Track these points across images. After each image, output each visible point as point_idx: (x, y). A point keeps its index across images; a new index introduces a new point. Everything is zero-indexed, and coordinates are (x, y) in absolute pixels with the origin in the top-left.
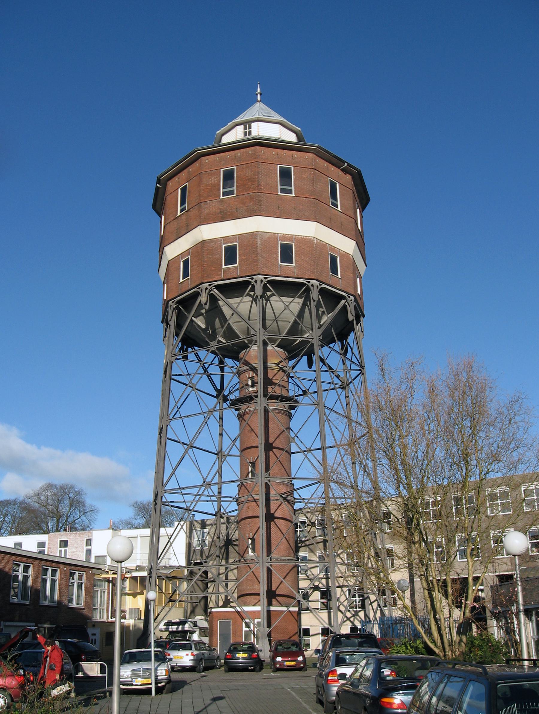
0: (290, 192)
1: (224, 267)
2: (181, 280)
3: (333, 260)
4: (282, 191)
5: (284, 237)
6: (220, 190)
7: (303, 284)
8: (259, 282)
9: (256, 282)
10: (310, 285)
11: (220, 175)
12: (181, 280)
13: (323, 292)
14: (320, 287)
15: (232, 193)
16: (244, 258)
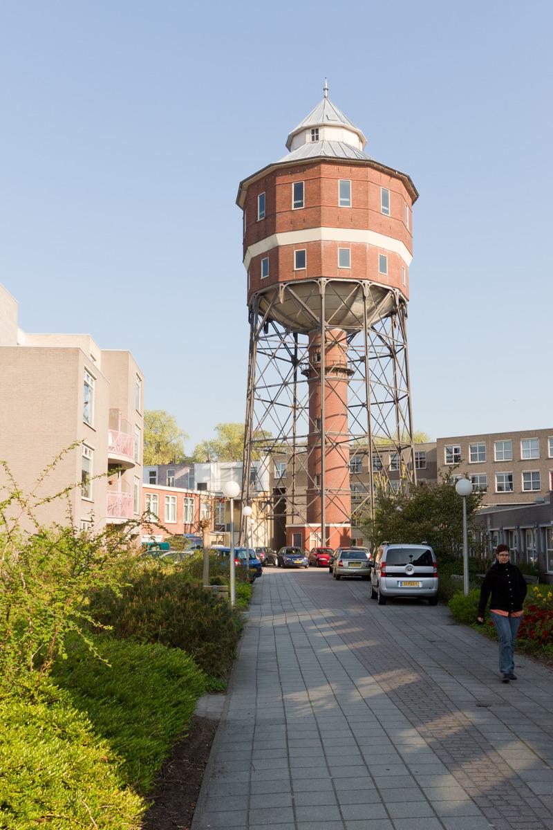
0: (348, 203)
1: (295, 269)
2: (262, 278)
3: (383, 260)
4: (343, 203)
5: (343, 244)
6: (291, 201)
7: (357, 283)
8: (323, 283)
9: (320, 282)
10: (362, 284)
11: (291, 188)
12: (262, 278)
13: (374, 288)
14: (370, 285)
15: (301, 205)
16: (311, 262)
